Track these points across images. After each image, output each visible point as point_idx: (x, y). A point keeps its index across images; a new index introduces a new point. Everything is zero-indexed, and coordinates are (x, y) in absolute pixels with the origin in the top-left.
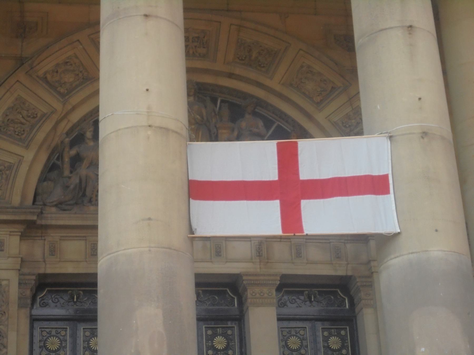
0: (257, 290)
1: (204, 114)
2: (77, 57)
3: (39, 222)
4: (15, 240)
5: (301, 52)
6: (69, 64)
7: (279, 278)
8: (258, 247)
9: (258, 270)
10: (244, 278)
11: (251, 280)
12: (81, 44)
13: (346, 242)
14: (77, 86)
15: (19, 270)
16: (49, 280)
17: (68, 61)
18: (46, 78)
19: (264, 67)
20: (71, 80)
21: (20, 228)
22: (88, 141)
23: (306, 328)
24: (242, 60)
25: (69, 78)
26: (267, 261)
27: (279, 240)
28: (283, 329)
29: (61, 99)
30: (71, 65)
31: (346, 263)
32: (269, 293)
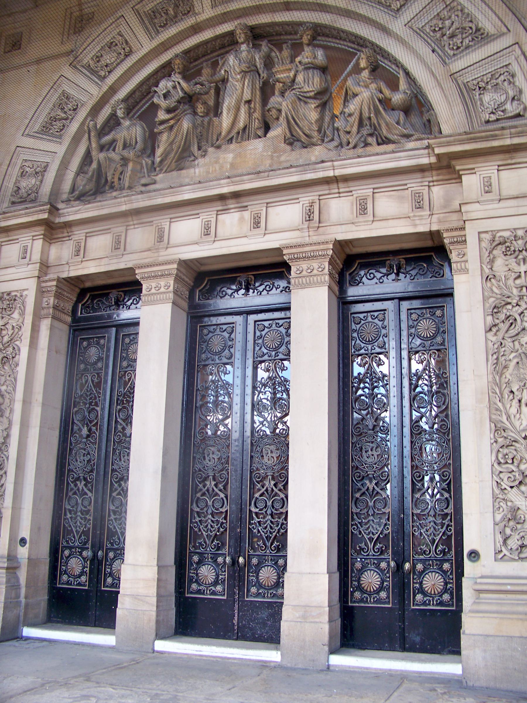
0: (304, 265)
2: (122, 36)
3: (57, 220)
4: (39, 244)
6: (114, 44)
7: (331, 246)
8: (308, 209)
9: (307, 238)
11: (294, 254)
13: (431, 184)
15: (39, 277)
16: (88, 284)
21: (40, 230)
22: (122, 121)
23: (386, 310)
26: (317, 225)
27: (337, 195)
28: (355, 315)
31: (429, 213)
32: (319, 267)
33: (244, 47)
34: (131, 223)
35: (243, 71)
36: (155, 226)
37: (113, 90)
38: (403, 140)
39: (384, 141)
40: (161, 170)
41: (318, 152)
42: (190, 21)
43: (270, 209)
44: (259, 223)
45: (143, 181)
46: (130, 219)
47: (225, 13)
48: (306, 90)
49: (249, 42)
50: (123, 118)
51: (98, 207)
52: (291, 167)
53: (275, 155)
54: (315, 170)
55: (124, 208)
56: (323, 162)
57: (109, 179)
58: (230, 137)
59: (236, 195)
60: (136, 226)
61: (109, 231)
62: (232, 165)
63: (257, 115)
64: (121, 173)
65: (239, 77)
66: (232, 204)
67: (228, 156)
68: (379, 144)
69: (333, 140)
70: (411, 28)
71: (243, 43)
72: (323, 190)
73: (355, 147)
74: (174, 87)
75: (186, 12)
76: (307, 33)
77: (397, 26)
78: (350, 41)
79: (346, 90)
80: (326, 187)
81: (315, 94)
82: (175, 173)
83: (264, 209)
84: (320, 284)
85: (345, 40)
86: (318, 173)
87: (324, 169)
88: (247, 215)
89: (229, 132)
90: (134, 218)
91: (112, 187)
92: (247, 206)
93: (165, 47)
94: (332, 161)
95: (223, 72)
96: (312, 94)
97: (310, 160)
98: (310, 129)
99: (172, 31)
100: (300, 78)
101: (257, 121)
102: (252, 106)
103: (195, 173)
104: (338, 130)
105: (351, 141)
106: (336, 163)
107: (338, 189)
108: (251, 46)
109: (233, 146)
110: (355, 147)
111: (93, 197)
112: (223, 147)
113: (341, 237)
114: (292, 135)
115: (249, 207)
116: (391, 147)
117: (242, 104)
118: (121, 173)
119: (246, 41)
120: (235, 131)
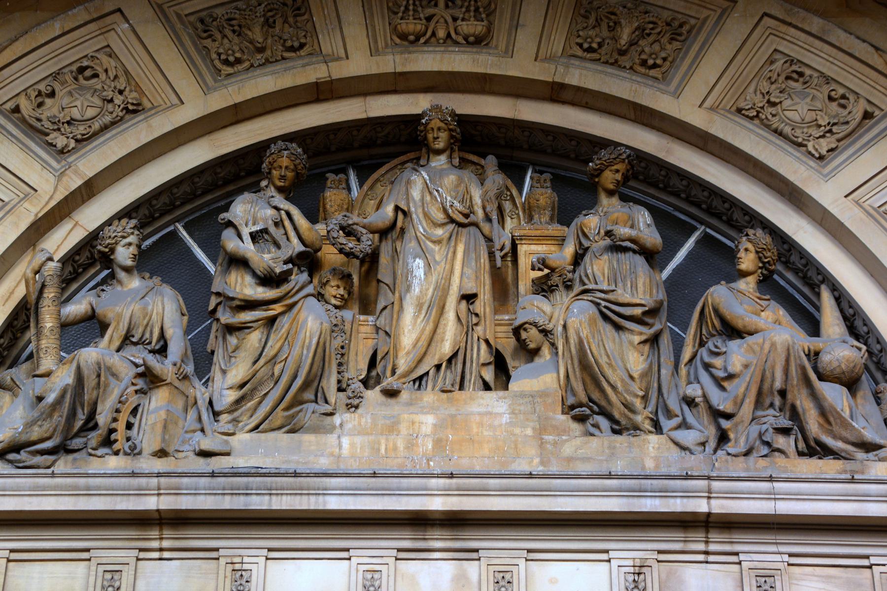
1: (478, 201)
5: (767, 21)
6: (88, 73)
8: (631, 578)
12: (127, 21)
14: (105, 128)
17: (85, 63)
18: (17, 110)
19: (655, 66)
20: (90, 113)
22: (122, 275)
24: (590, 50)
25: (82, 106)
27: (701, 557)
29: (54, 163)
30: (96, 76)
33: (440, 162)
34: (155, 544)
35: (452, 221)
36: (222, 561)
37: (89, 190)
38: (860, 455)
39: (815, 450)
40: (235, 421)
41: (652, 451)
42: (315, 73)
45: (207, 444)
46: (155, 533)
47: (402, 74)
48: (621, 300)
49: (452, 151)
50: (127, 270)
51: (76, 488)
52: (610, 476)
53: (549, 438)
54: (664, 494)
55: (151, 503)
56: (687, 477)
57: (103, 419)
58: (420, 372)
59: (455, 521)
60: (166, 555)
61: (85, 555)
62: (439, 443)
64: (134, 411)
65: (439, 232)
66: (438, 540)
67: (422, 419)
68: (801, 454)
69: (684, 425)
70: (857, 202)
71: (439, 152)
72: (672, 540)
73: (747, 454)
74: (278, 224)
75: (296, 44)
76: (615, 167)
77: (828, 193)
78: (688, 200)
79: (702, 312)
80: (679, 535)
81: (645, 313)
82: (281, 437)
85: (677, 195)
86: (672, 501)
87: (687, 494)
90: (167, 533)
91: (107, 442)
92: (476, 550)
93: (237, 114)
94: (709, 478)
95: (389, 210)
96: (638, 311)
97: (643, 468)
98: (628, 391)
99: (264, 83)
100: (599, 267)
101: (483, 346)
103: (340, 446)
104: (690, 402)
105: (732, 436)
106: (716, 485)
107: (707, 542)
108: (456, 161)
109: (429, 396)
110: (747, 454)
111: (51, 458)
112: (404, 396)
114: (591, 400)
116: (829, 467)
118: (134, 411)
119: (449, 149)
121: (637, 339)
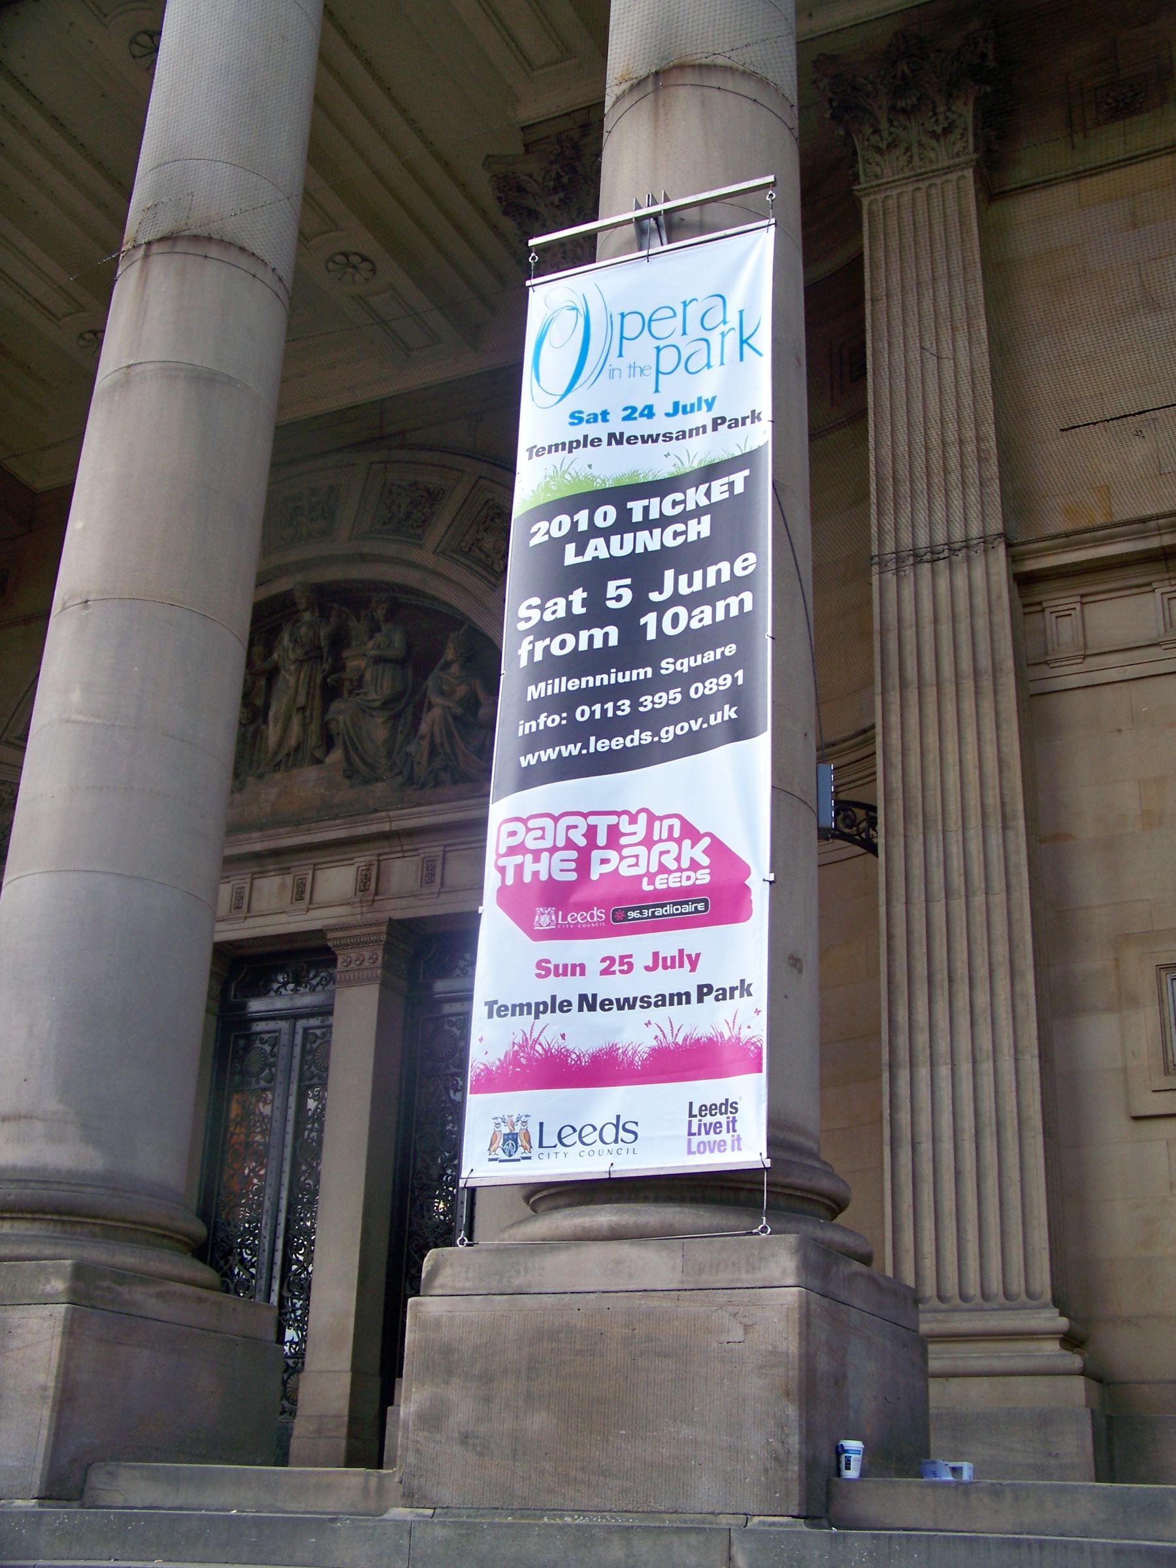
5: (482, 482)
7: (384, 928)
9: (359, 917)
10: (330, 935)
27: (400, 855)
43: (318, 873)
44: (303, 892)
63: (314, 728)
83: (311, 872)
84: (369, 980)
87: (380, 821)
88: (289, 879)
89: (276, 753)
102: (308, 713)
109: (278, 776)
110: (422, 787)
113: (398, 915)
115: (292, 870)
117: (294, 714)
120: (284, 751)
121: (381, 720)
